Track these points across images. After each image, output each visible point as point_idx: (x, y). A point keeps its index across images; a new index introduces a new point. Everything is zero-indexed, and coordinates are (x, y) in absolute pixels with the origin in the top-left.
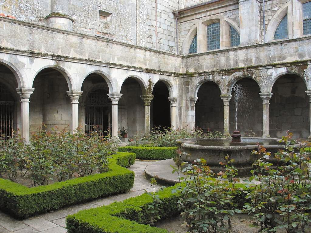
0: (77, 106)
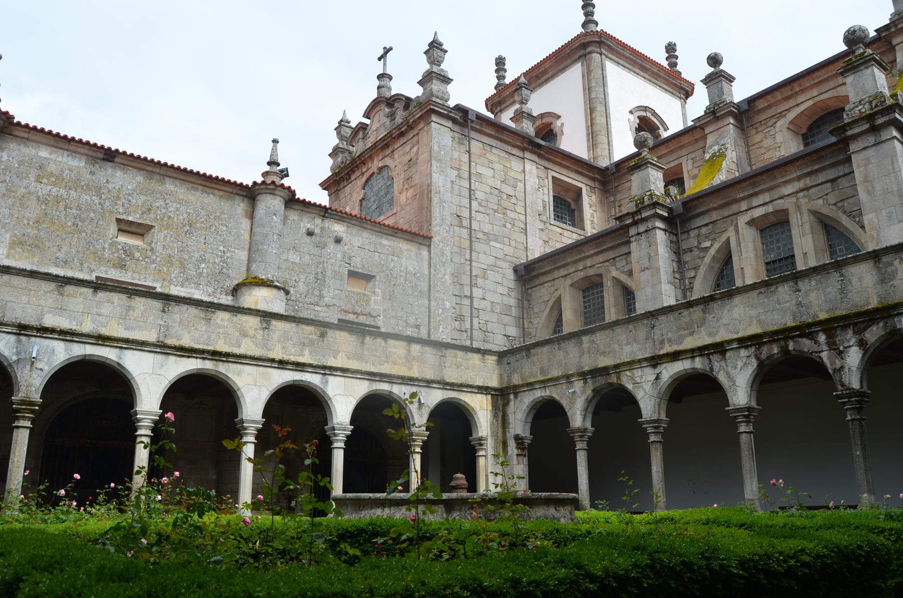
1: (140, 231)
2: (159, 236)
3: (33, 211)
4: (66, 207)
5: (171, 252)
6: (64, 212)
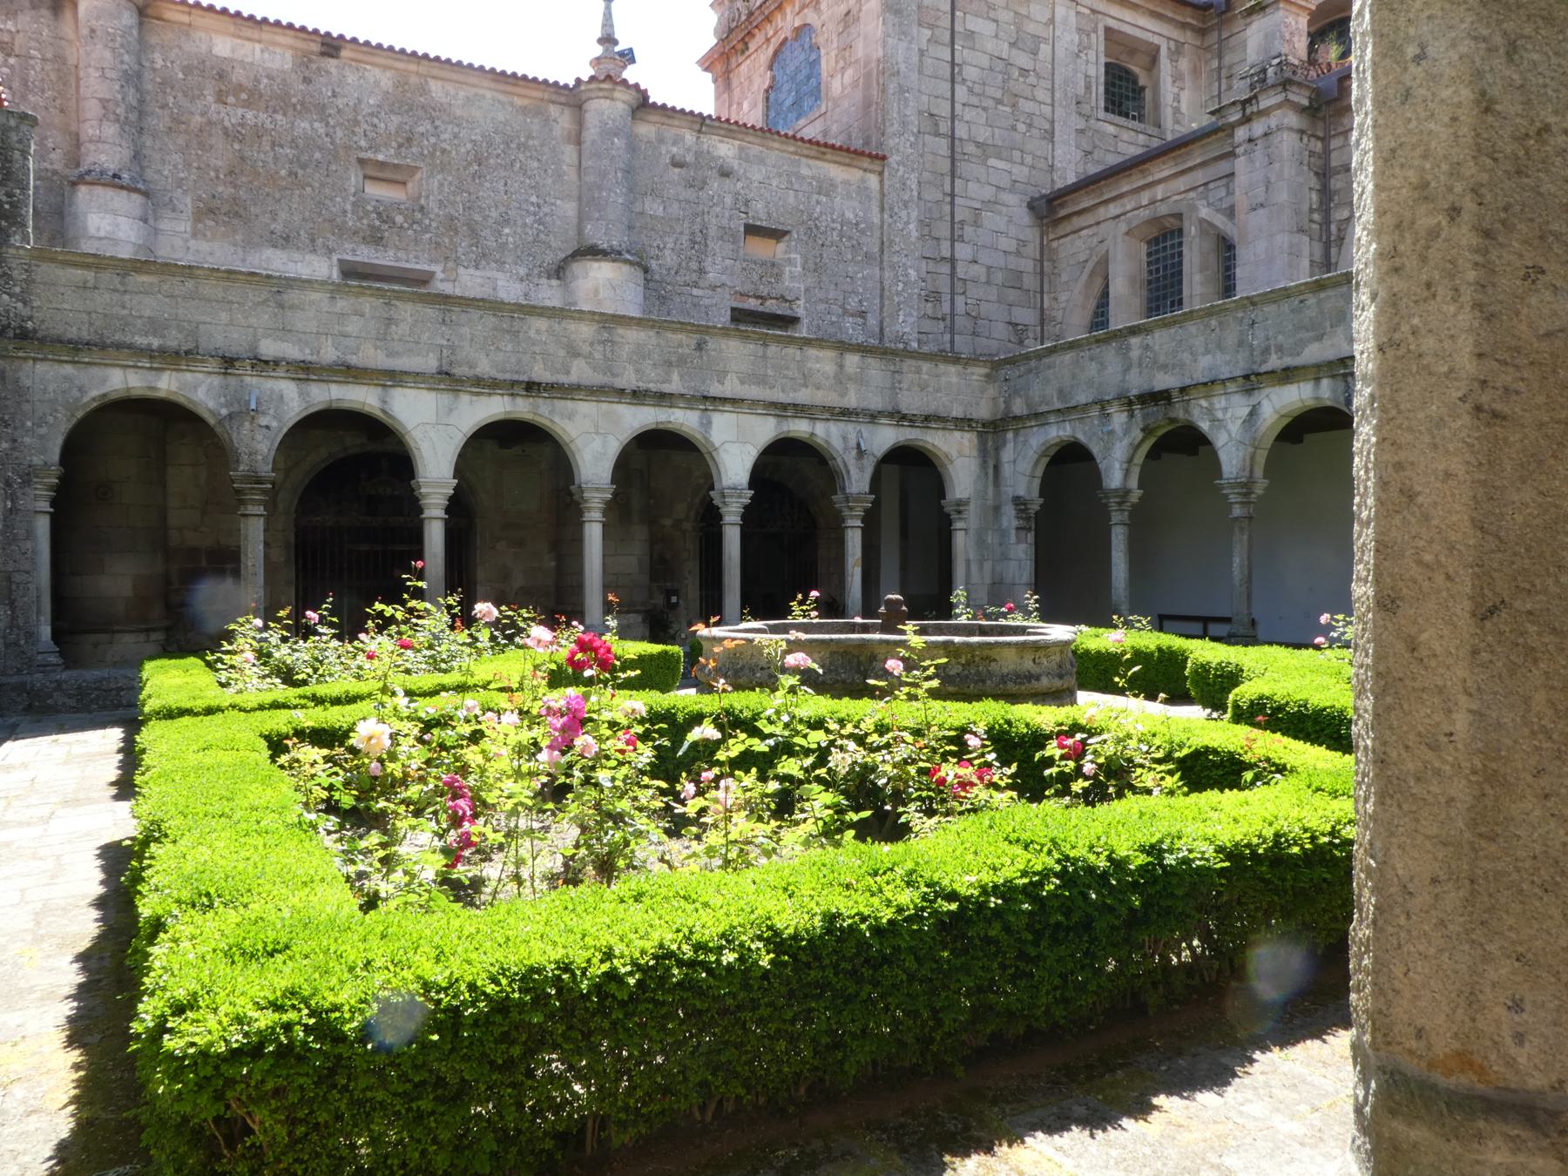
0: (858, 533)
1: (398, 177)
4: (273, 144)
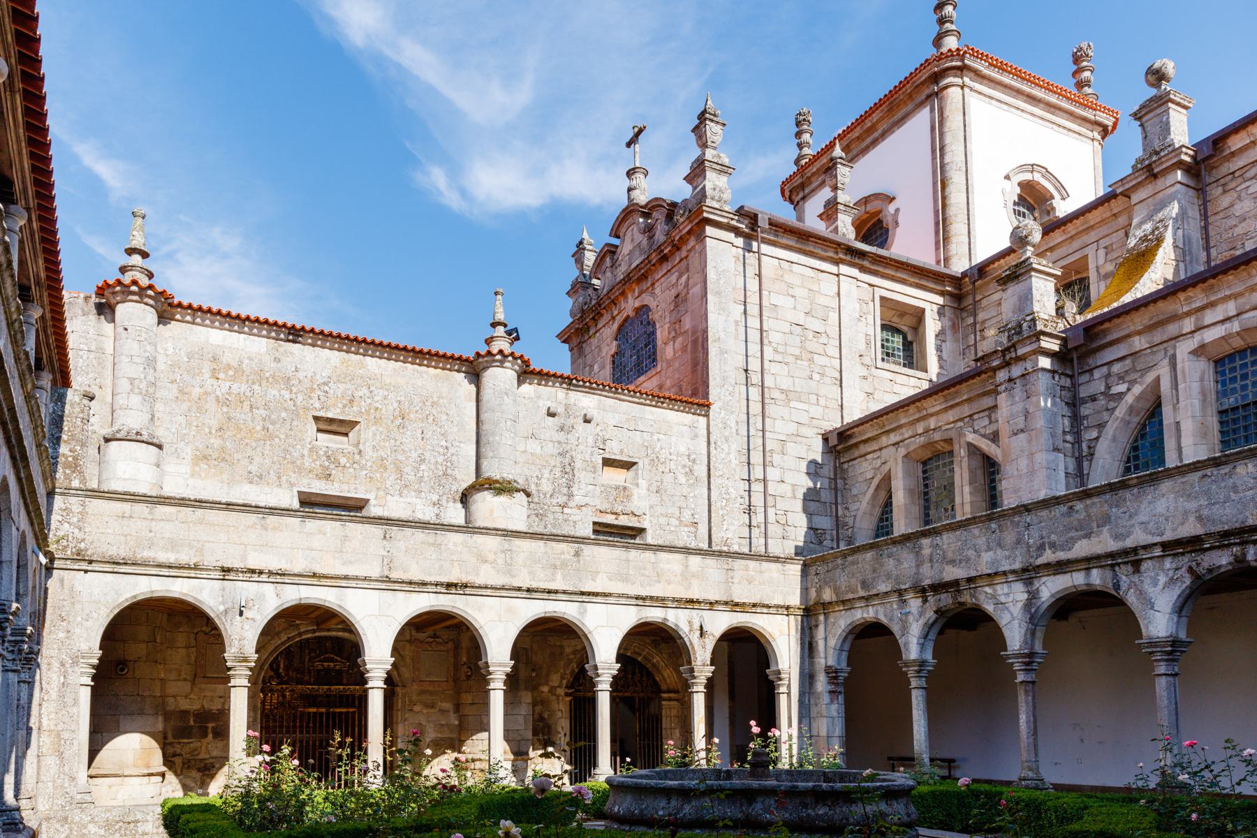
1: (342, 430)
2: (366, 434)
3: (213, 417)
4: (251, 407)
5: (383, 454)
6: (250, 414)
